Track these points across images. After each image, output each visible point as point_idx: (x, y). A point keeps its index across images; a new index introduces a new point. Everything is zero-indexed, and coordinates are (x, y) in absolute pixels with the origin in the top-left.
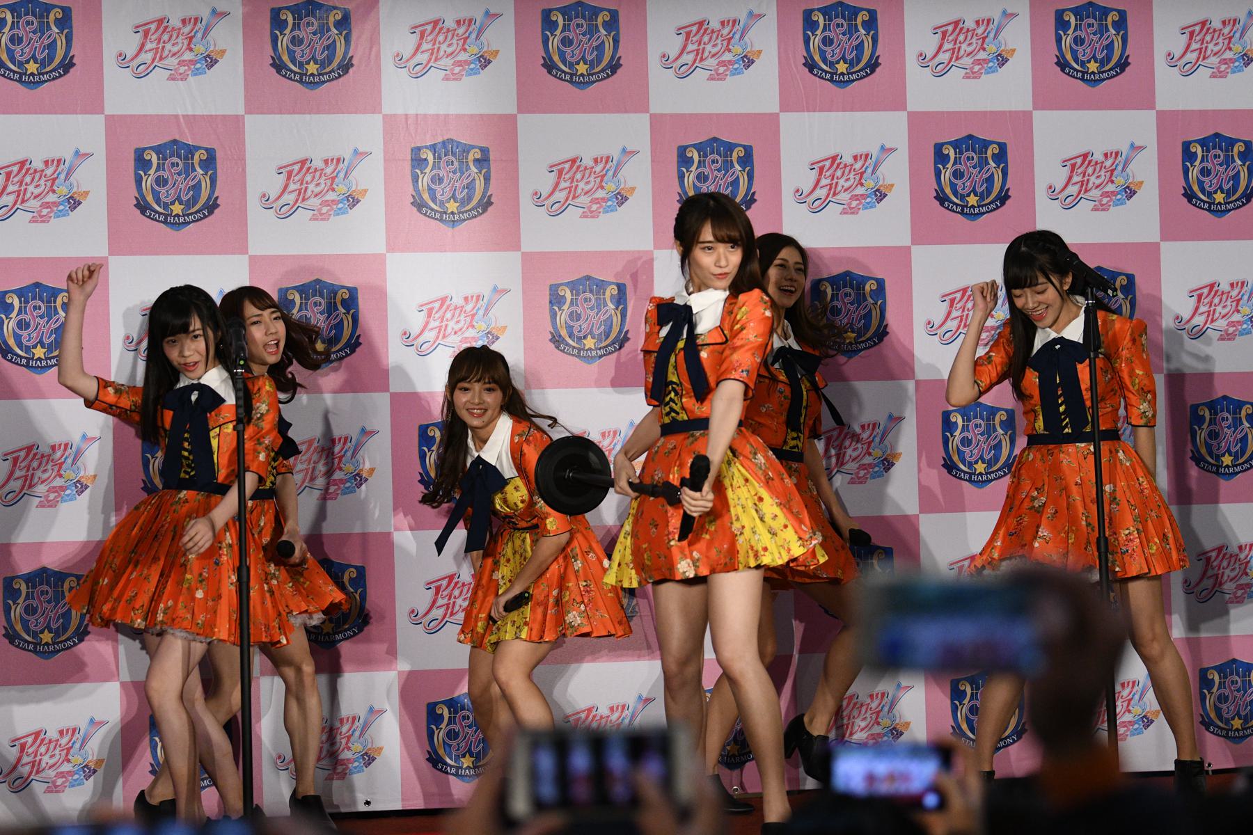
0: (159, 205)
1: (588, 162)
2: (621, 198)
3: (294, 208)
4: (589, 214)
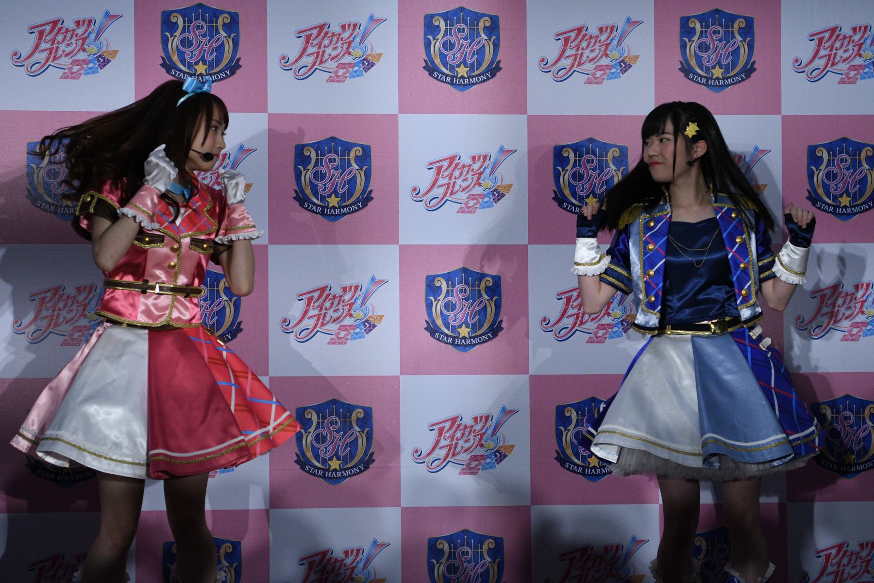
0: (184, 64)
1: (593, 31)
2: (625, 66)
3: (312, 70)
4: (593, 80)
